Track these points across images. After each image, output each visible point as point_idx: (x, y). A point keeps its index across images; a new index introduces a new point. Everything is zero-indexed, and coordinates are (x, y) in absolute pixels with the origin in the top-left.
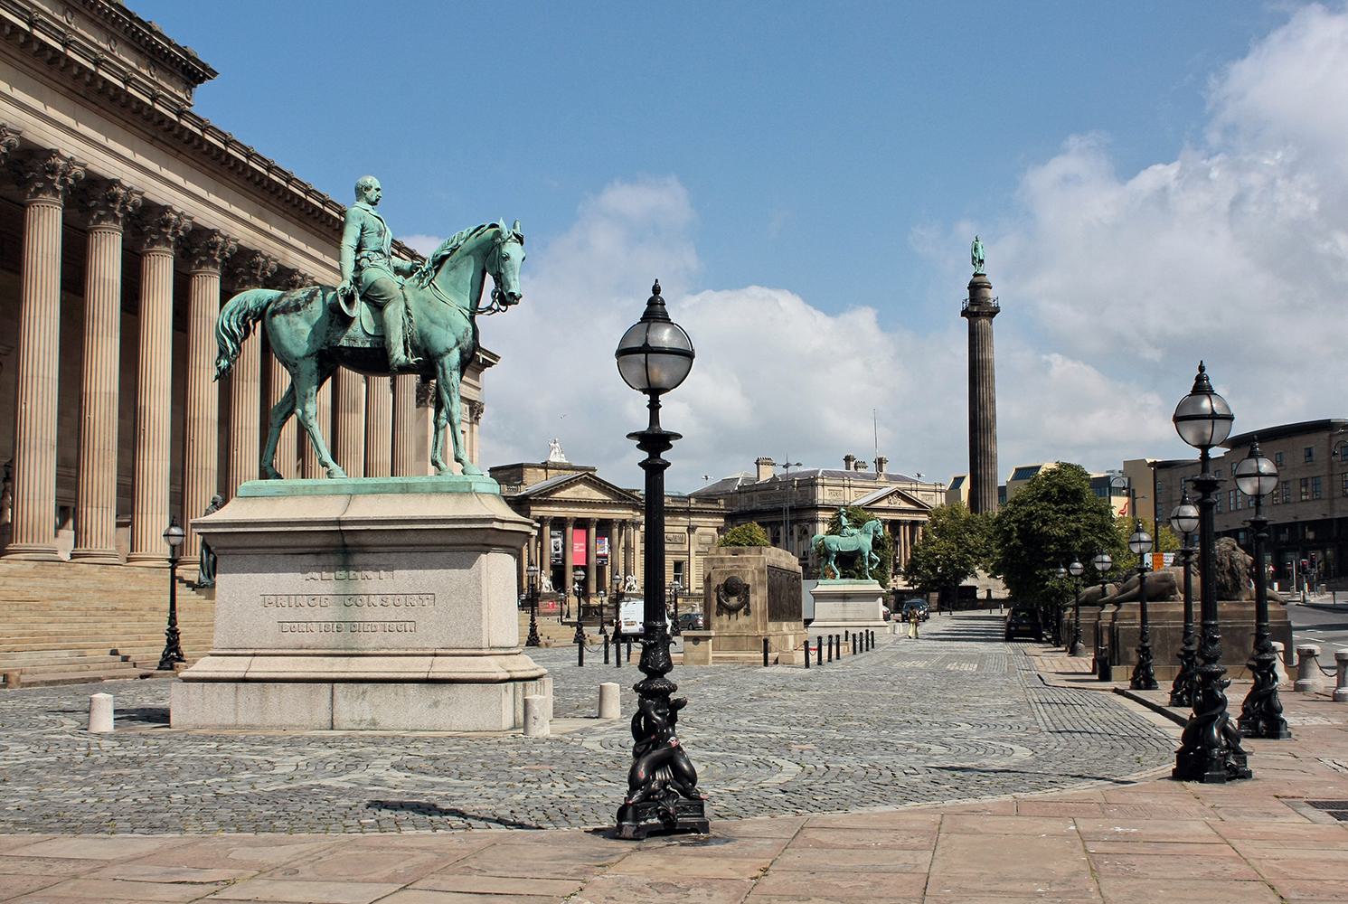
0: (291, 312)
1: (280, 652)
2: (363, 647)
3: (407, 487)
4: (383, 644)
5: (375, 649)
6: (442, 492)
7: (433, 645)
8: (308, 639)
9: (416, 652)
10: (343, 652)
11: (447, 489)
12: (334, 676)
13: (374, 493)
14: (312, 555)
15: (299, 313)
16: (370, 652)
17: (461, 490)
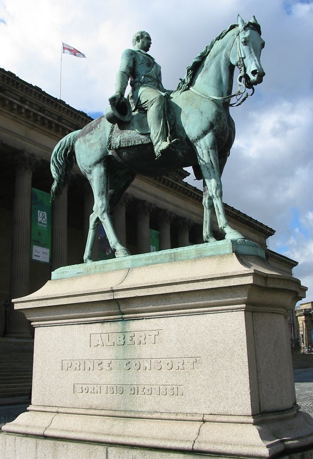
0: (87, 133)
1: (75, 411)
2: (140, 410)
3: (175, 256)
4: (156, 407)
5: (149, 412)
6: (206, 257)
7: (203, 409)
8: (95, 400)
9: (185, 418)
10: (122, 414)
11: (210, 253)
12: (110, 439)
13: (147, 265)
14: (98, 324)
15: (92, 132)
16: (144, 416)
17: (222, 253)
